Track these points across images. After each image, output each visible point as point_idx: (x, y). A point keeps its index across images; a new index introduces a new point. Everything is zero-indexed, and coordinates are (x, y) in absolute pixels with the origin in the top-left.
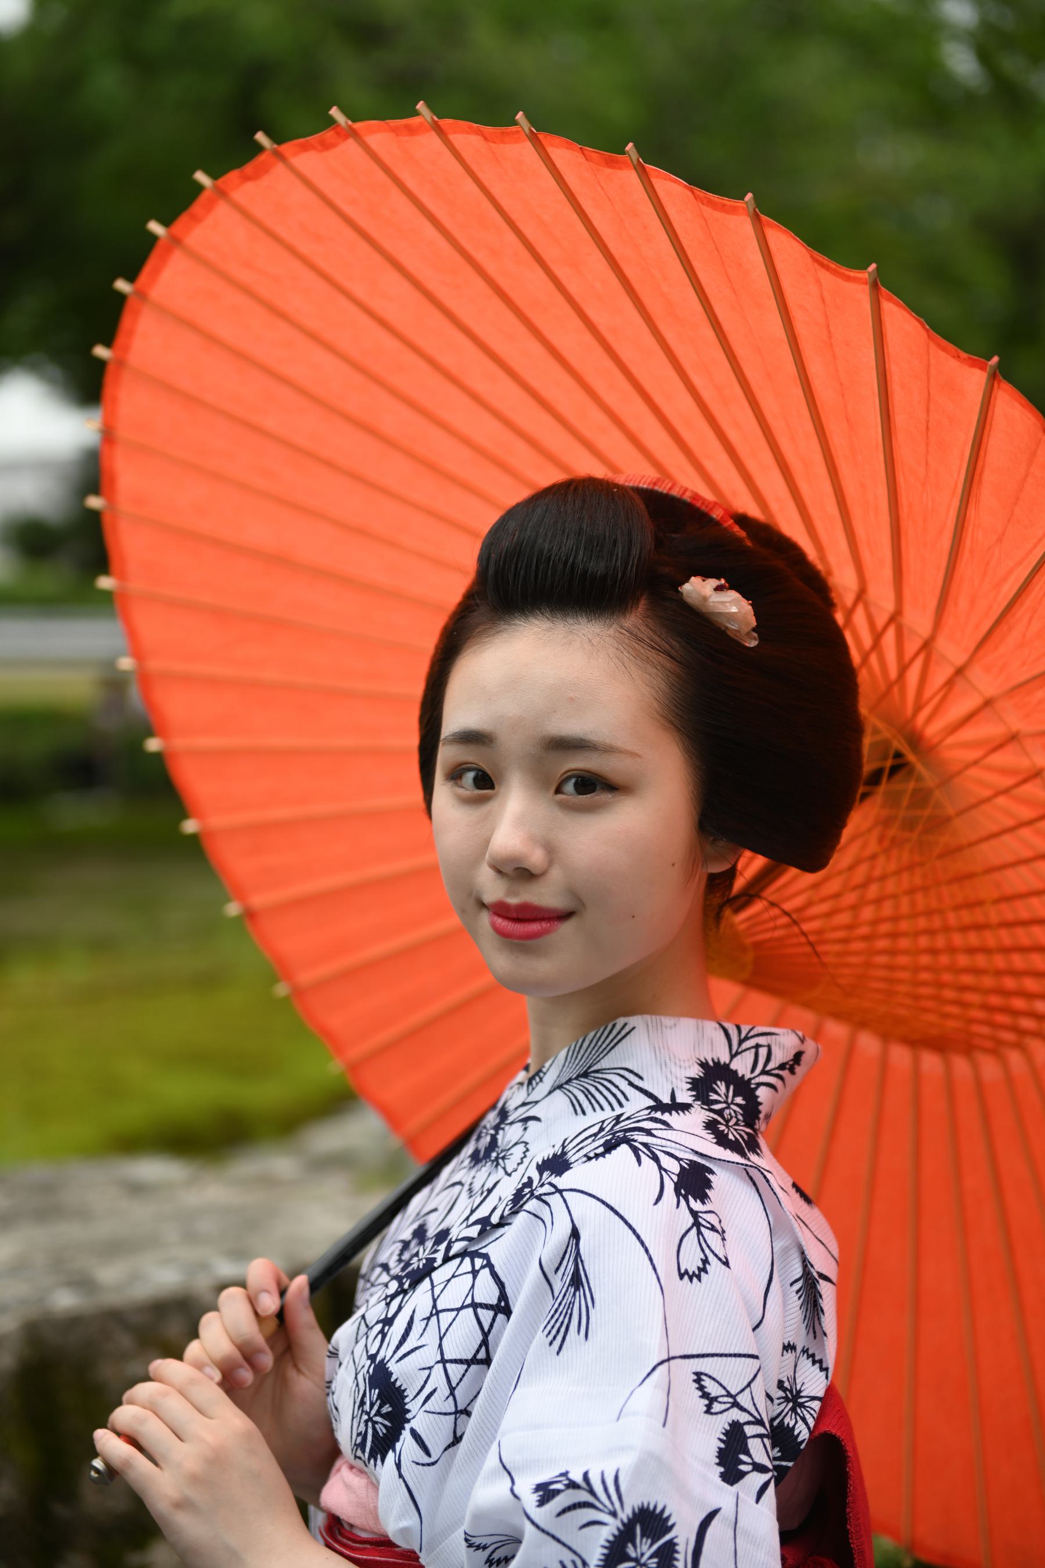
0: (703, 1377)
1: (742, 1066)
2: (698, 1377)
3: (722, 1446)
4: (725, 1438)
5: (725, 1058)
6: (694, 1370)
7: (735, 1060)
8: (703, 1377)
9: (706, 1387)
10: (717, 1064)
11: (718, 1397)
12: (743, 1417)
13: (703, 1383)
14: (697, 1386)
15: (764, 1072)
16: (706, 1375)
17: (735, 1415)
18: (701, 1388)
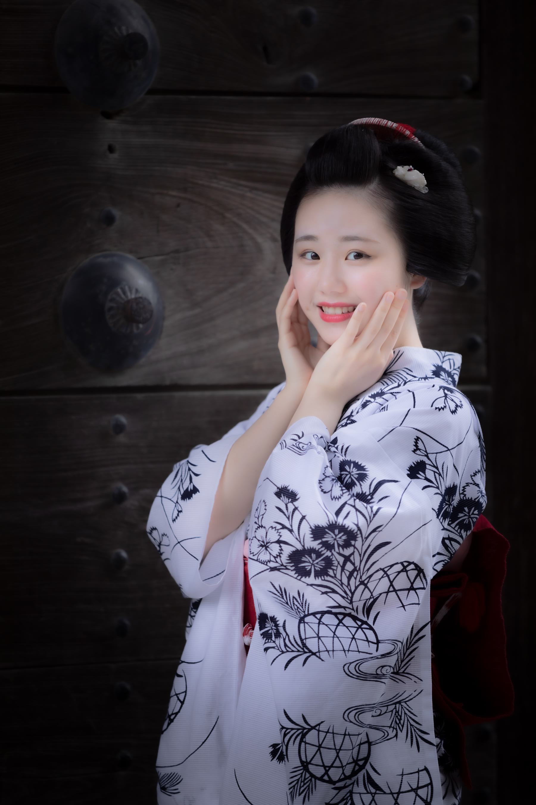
0: (419, 440)
1: (446, 366)
2: (417, 439)
3: (413, 465)
4: (416, 464)
5: (440, 364)
6: (417, 436)
7: (444, 364)
8: (419, 440)
9: (418, 443)
10: (438, 365)
11: (421, 449)
12: (427, 461)
13: (418, 441)
14: (415, 441)
15: (454, 369)
16: (421, 440)
17: (425, 459)
18: (416, 443)
